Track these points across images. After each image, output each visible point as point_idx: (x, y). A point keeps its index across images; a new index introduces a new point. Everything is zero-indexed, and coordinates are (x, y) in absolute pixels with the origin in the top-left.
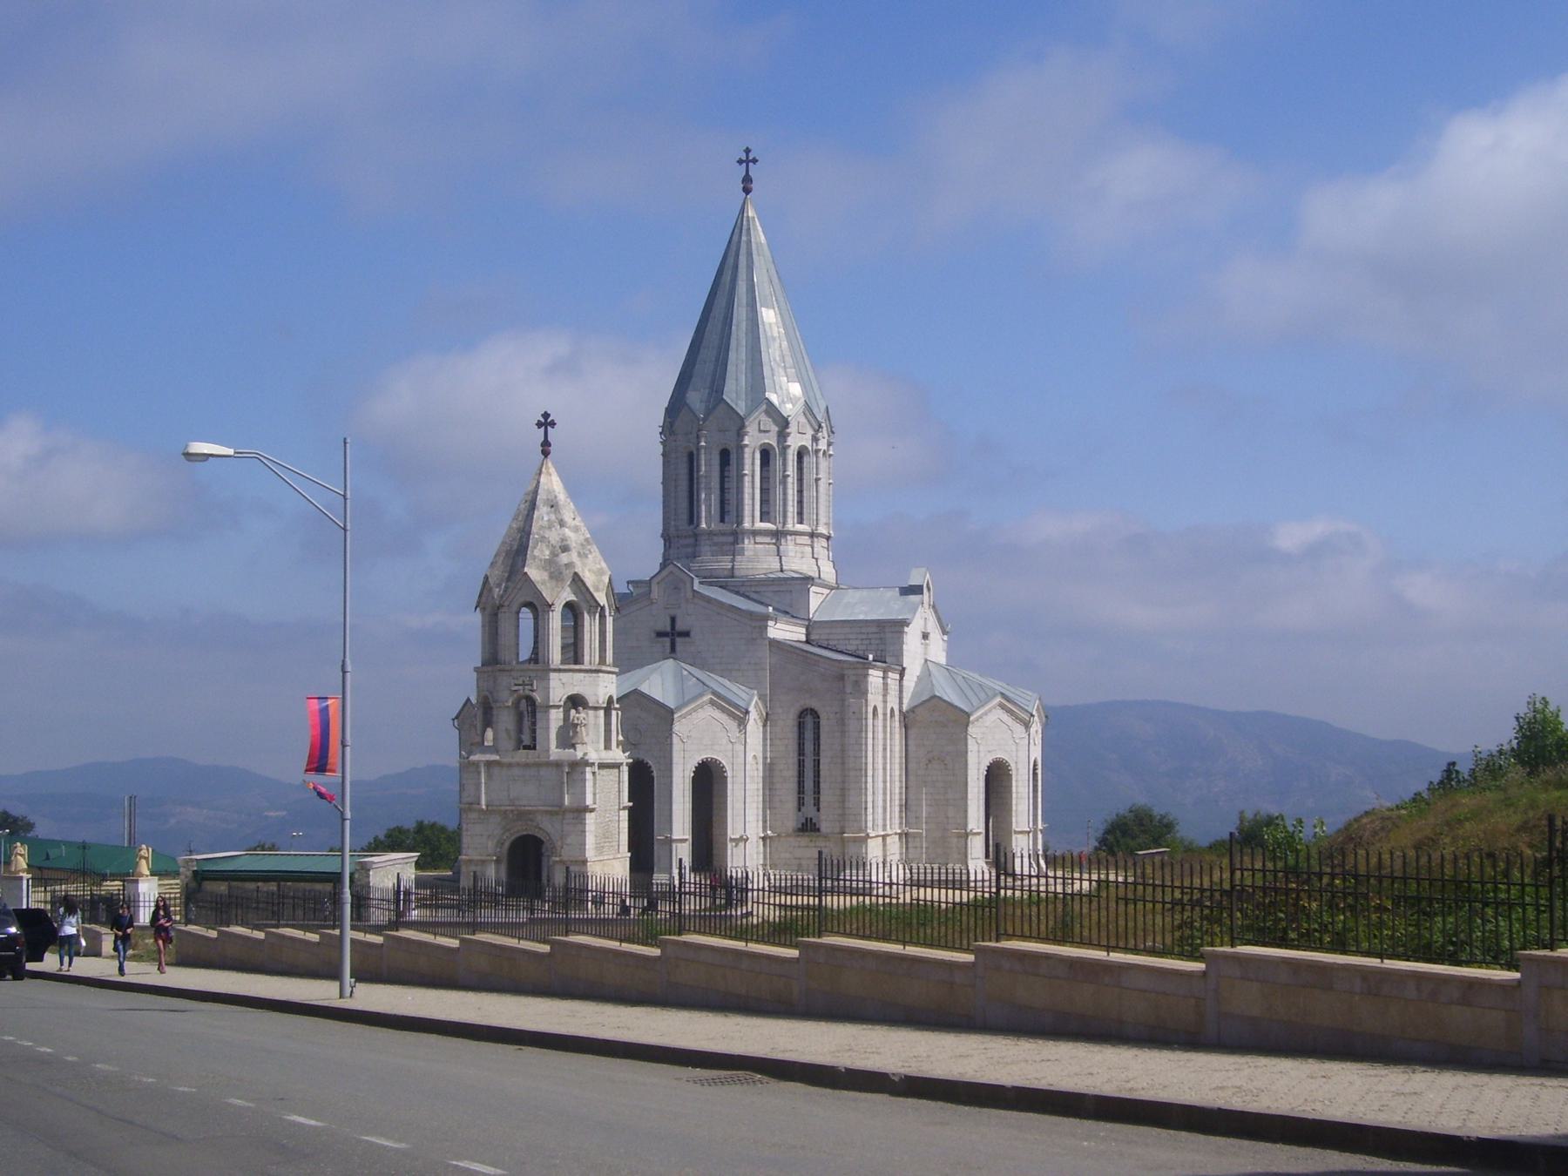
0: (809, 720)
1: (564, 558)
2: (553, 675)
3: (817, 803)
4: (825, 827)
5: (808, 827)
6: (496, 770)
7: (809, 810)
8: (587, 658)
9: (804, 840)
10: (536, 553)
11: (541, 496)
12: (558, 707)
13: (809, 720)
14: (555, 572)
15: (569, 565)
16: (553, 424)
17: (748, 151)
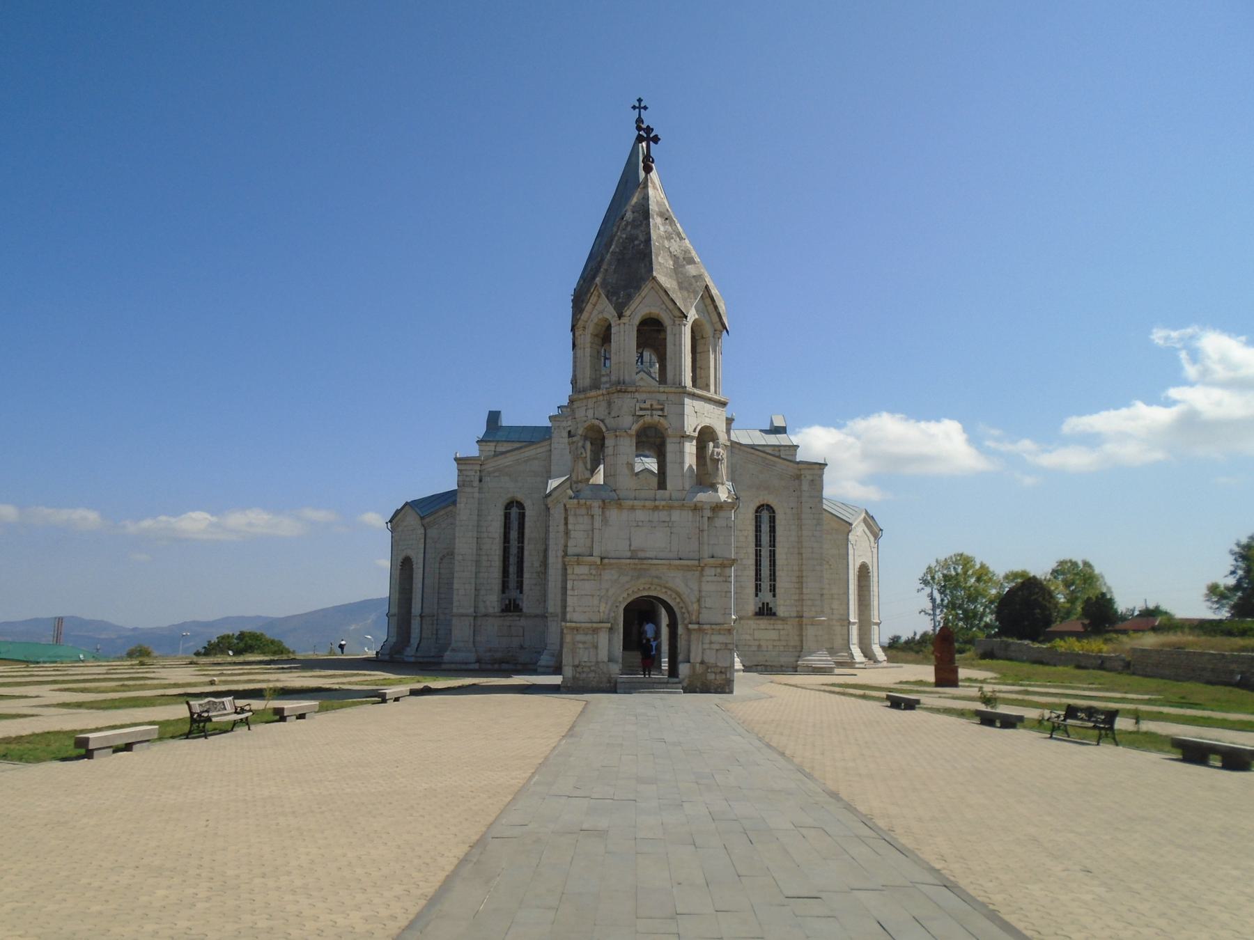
0: (765, 515)
1: (691, 270)
2: (687, 401)
3: (773, 589)
4: (781, 611)
5: (765, 611)
6: (613, 514)
7: (766, 596)
8: (712, 388)
9: (763, 623)
10: (660, 260)
11: (653, 207)
12: (690, 438)
13: (765, 515)
14: (687, 283)
15: (699, 277)
16: (656, 139)
17: (640, 100)
